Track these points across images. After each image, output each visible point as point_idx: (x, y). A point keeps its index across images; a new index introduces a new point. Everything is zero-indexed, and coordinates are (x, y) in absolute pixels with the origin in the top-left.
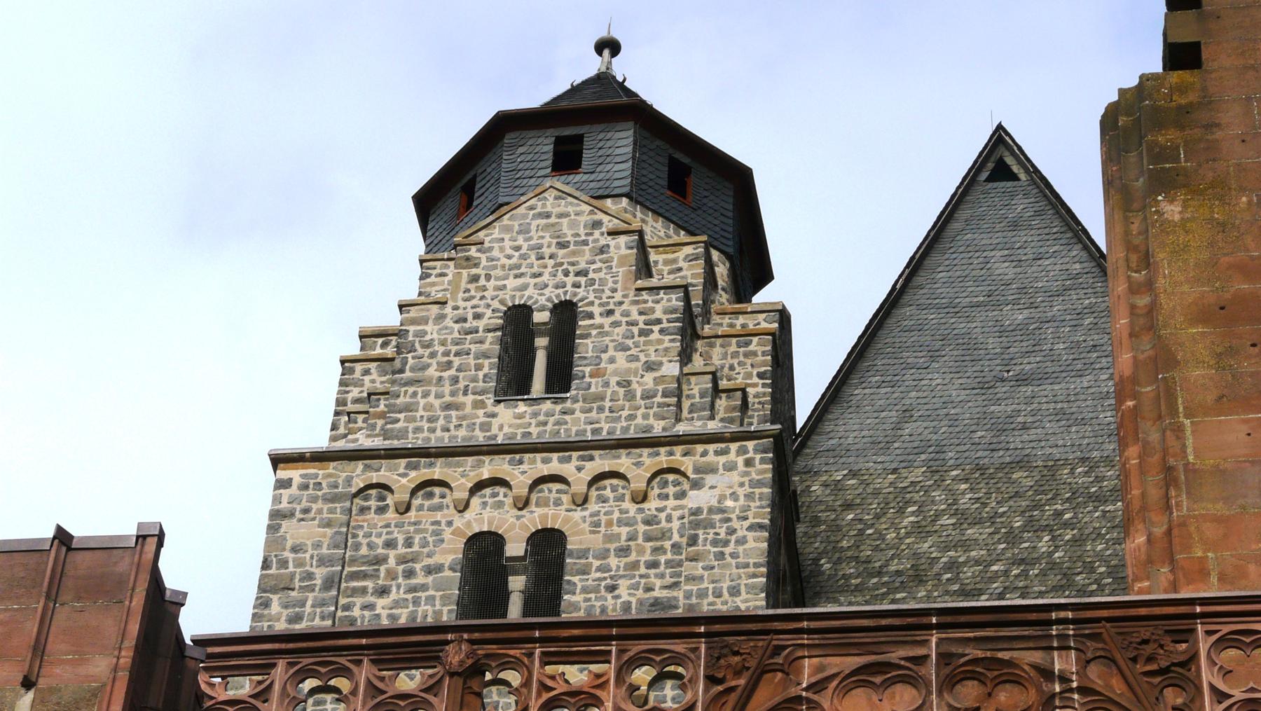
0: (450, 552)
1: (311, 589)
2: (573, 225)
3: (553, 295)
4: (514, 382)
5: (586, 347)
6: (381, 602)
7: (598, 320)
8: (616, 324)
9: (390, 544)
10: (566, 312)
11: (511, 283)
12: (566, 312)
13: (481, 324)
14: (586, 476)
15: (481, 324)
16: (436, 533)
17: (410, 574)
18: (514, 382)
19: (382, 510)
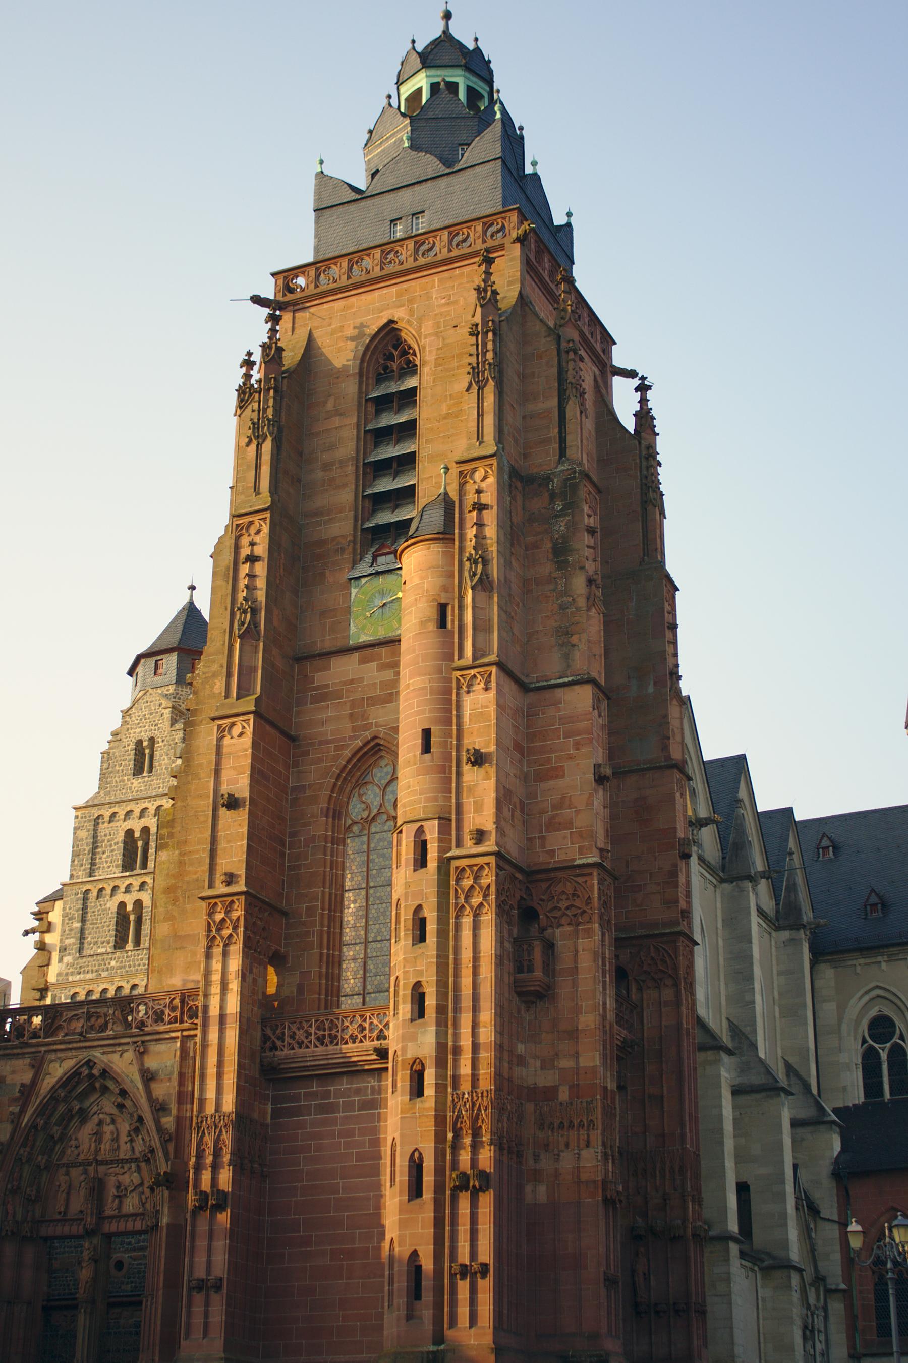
0: (121, 837)
1: (84, 854)
2: (155, 705)
3: (149, 734)
4: (138, 770)
5: (157, 754)
6: (104, 856)
7: (161, 744)
8: (165, 745)
9: (105, 835)
10: (152, 740)
11: (138, 730)
12: (152, 740)
13: (129, 748)
14: (154, 807)
15: (129, 748)
16: (117, 830)
17: (111, 846)
18: (138, 770)
19: (103, 823)
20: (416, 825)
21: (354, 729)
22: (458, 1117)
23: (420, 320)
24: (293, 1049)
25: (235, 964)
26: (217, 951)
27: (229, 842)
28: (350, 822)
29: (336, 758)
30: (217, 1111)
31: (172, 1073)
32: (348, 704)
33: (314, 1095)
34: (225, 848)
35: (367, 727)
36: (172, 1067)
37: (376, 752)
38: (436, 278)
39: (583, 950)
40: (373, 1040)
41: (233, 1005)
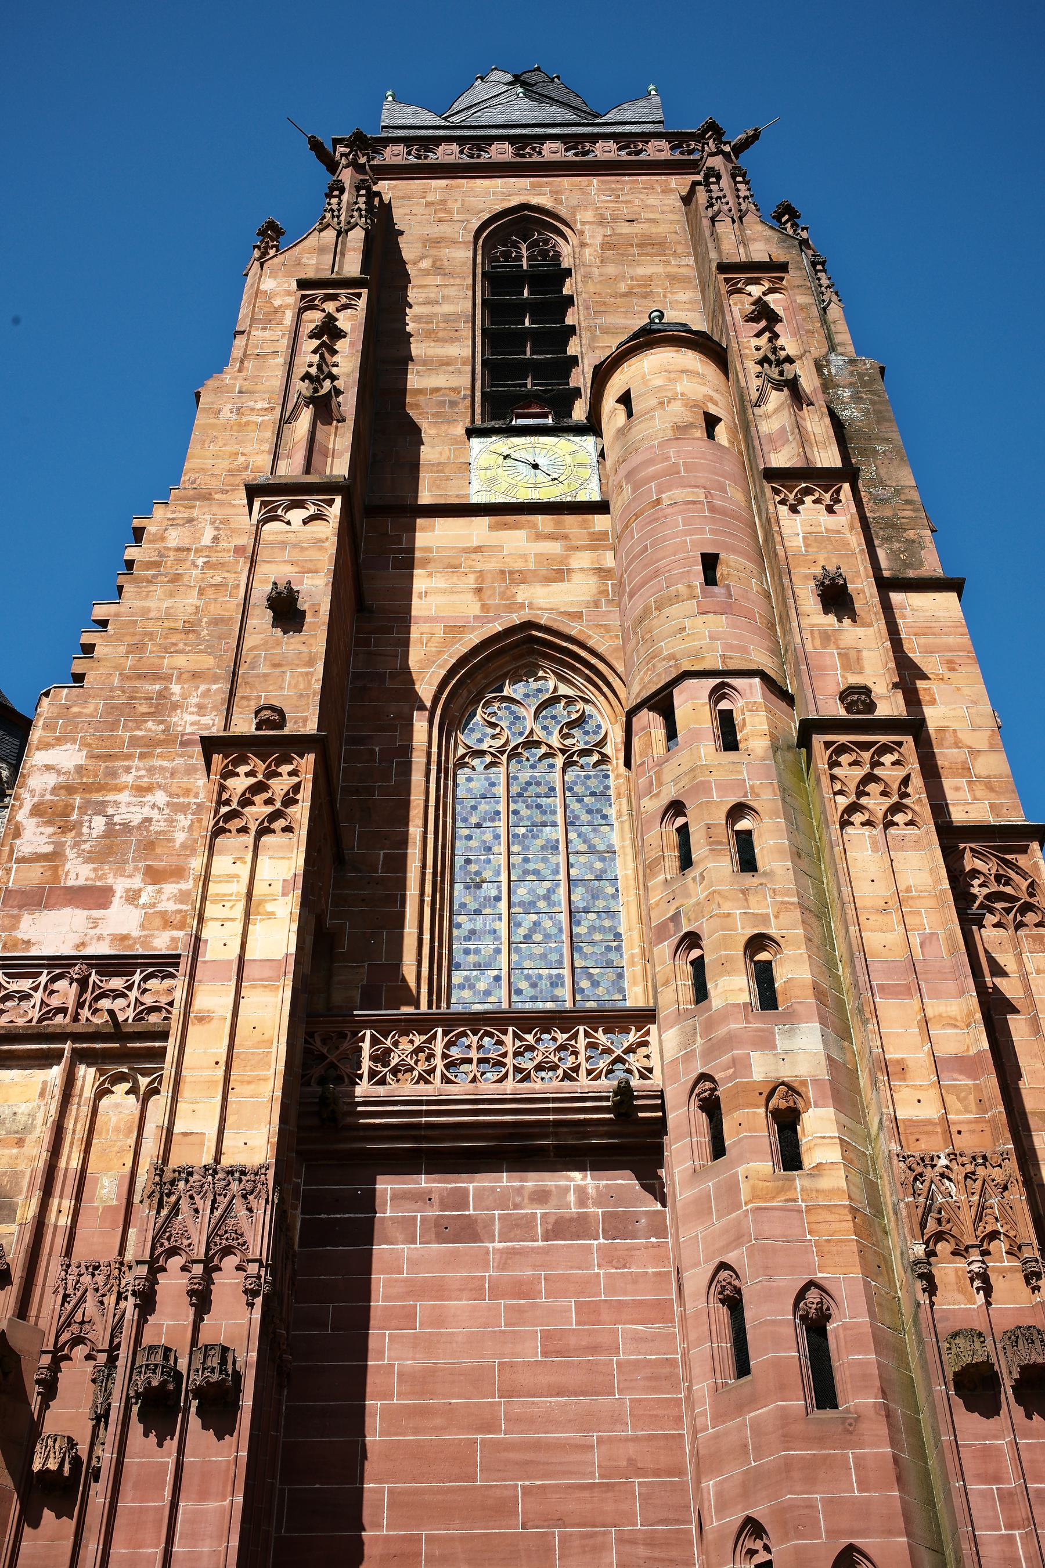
20: (714, 682)
21: (484, 607)
22: (927, 1210)
23: (574, 210)
24: (382, 1082)
25: (284, 861)
26: (234, 844)
27: (276, 666)
28: (461, 751)
29: (445, 645)
30: (217, 1160)
31: (27, 1129)
32: (472, 578)
33: (426, 1198)
34: (265, 675)
35: (513, 606)
36: (32, 1116)
37: (522, 656)
38: (595, 180)
39: (1038, 972)
40: (597, 1077)
41: (277, 936)
